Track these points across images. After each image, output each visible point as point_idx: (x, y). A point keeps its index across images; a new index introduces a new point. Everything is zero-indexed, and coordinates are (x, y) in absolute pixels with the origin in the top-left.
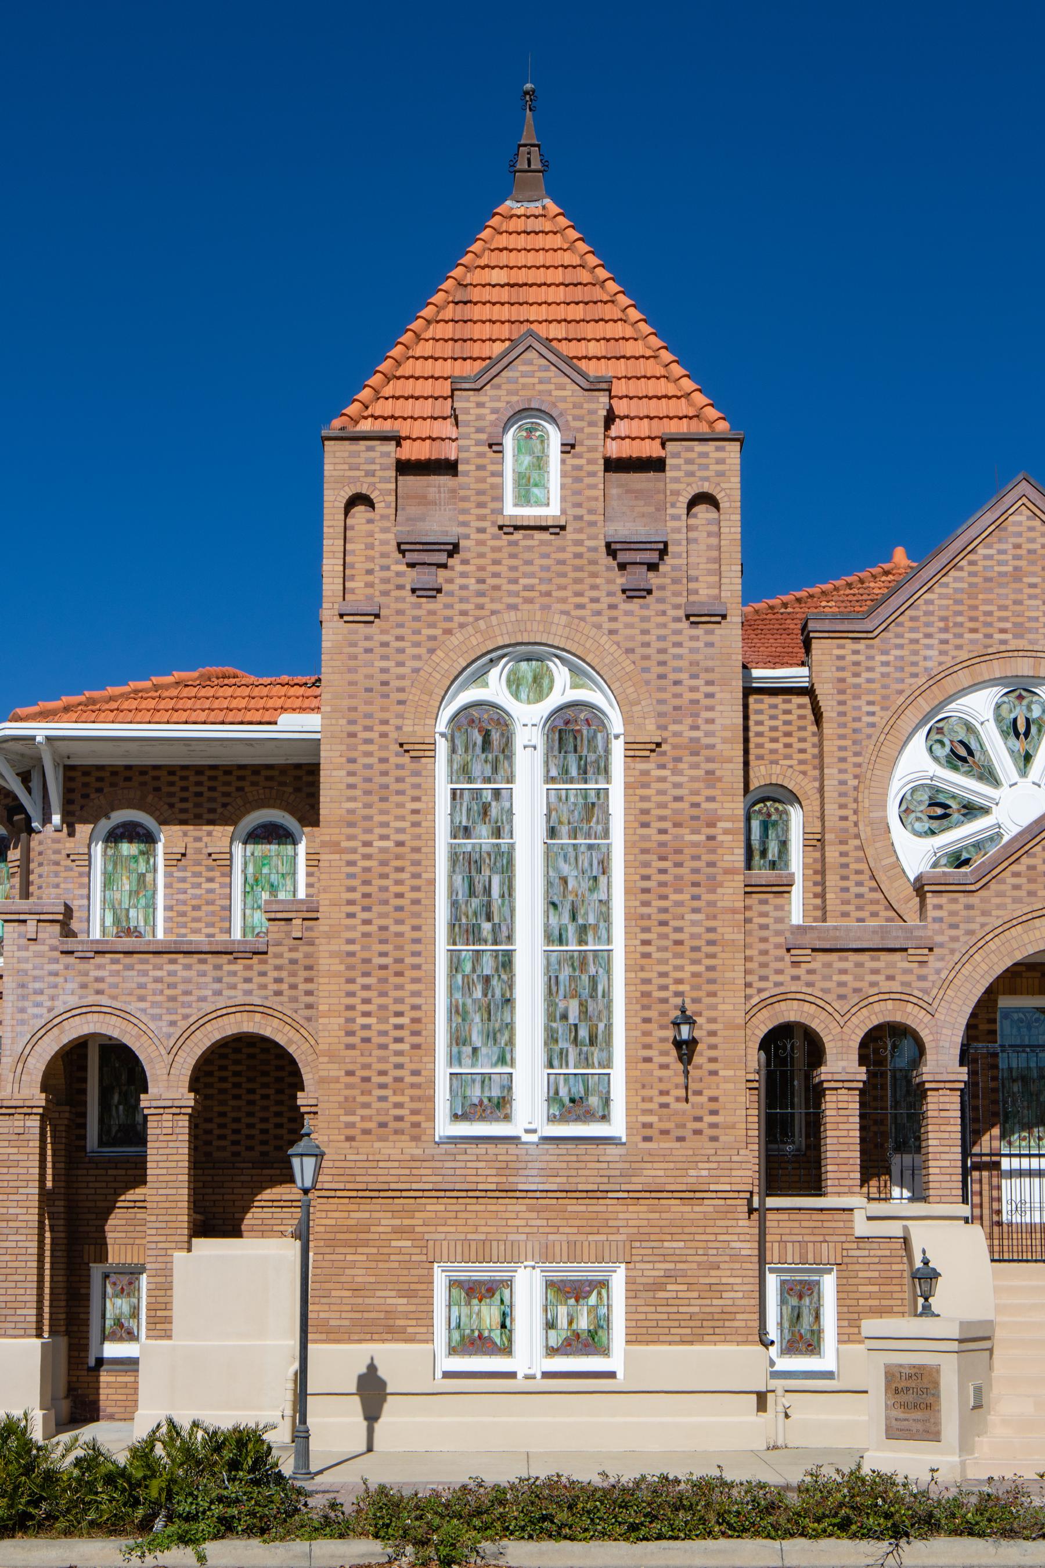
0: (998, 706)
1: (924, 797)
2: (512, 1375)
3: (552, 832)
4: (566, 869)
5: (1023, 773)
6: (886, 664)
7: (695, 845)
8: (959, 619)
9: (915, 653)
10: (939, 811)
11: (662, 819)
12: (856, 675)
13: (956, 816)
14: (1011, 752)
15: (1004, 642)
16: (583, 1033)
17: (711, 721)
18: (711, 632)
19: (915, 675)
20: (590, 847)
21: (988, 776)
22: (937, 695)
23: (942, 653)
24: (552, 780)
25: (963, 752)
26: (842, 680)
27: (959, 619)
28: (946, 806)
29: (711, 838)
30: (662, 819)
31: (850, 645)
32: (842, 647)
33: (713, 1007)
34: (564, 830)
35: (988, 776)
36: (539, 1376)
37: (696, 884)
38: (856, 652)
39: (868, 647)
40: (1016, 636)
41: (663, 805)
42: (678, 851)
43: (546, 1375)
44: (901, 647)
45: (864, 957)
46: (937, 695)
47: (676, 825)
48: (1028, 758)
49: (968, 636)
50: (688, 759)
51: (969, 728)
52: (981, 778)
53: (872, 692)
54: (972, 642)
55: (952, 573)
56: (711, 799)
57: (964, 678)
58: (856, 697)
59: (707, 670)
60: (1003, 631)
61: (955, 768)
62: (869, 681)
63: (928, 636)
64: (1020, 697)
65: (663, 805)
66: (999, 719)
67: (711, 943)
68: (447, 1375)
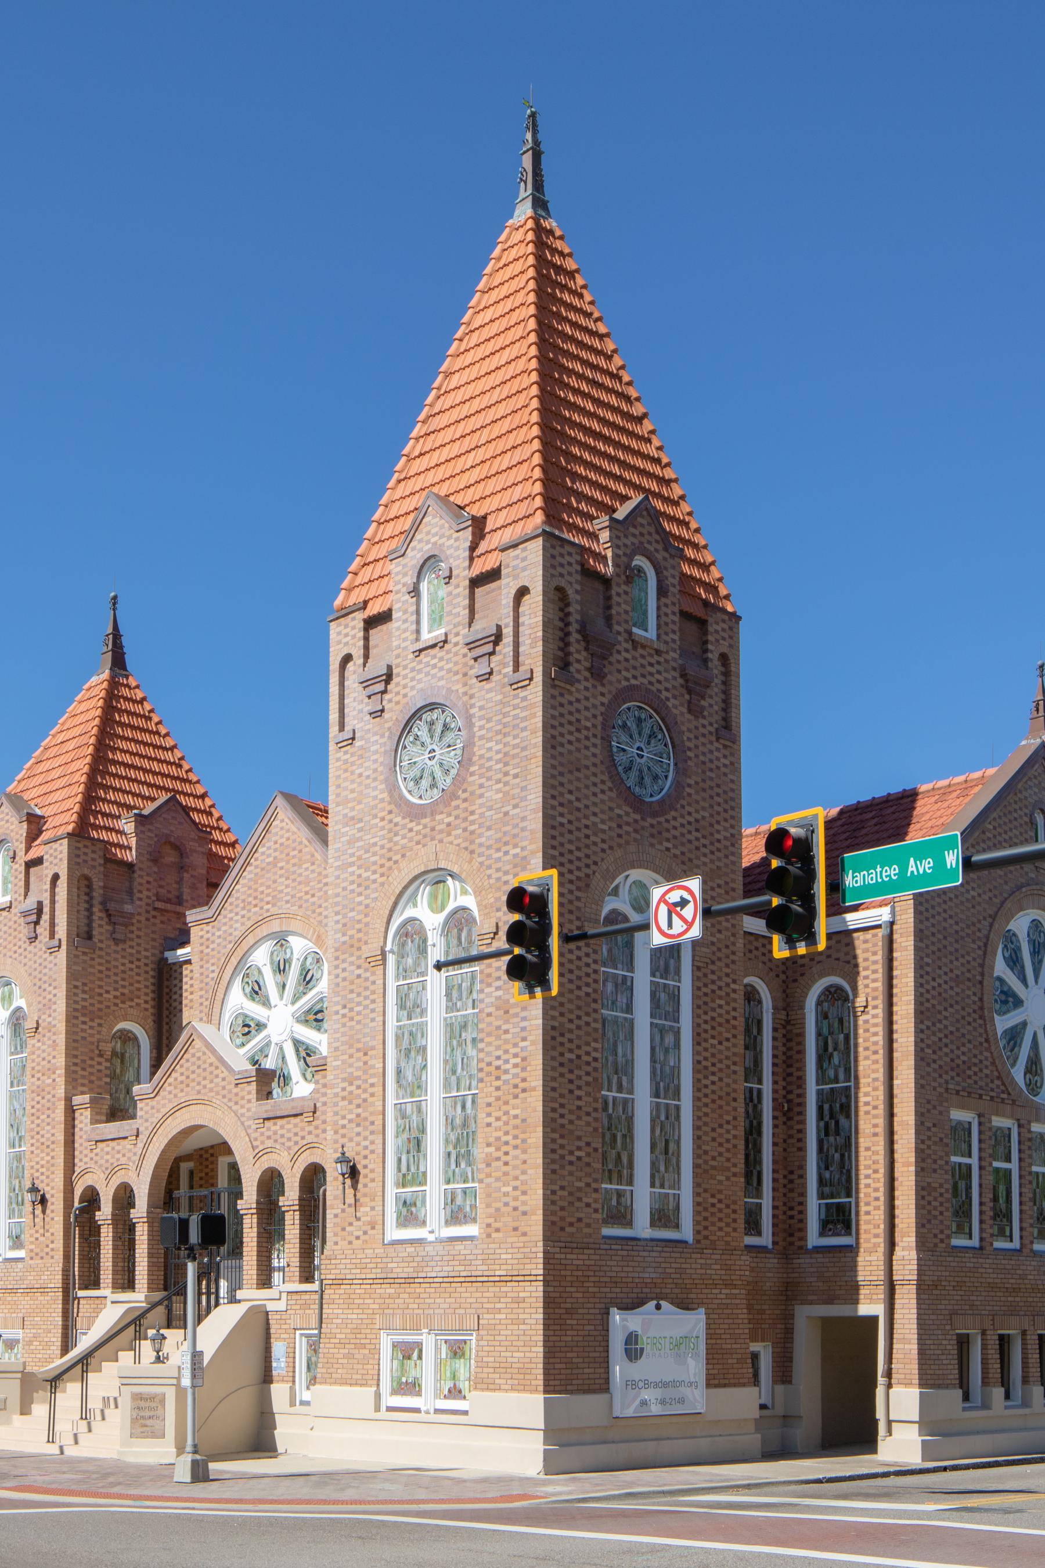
0: (272, 953)
1: (240, 1022)
2: (417, 1410)
3: (12, 1086)
4: (17, 1105)
5: (281, 997)
6: (219, 937)
7: (49, 1085)
8: (250, 899)
9: (231, 927)
10: (246, 1030)
11: (39, 1072)
12: (208, 947)
13: (253, 1032)
14: (277, 983)
15: (268, 911)
16: (20, 1199)
17: (55, 1011)
18: (56, 957)
19: (230, 942)
20: (23, 1090)
21: (266, 1003)
22: (239, 953)
23: (243, 924)
24: (12, 1054)
25: (257, 988)
26: (202, 952)
27: (250, 899)
28: (248, 1026)
29: (54, 1080)
30: (39, 1072)
31: (206, 928)
32: (202, 930)
33: (53, 1181)
34: (15, 1082)
35: (266, 1003)
36: (432, 1411)
37: (49, 1109)
38: (208, 932)
39: (213, 927)
40: (274, 905)
41: (39, 1064)
42: (43, 1090)
43: (437, 1411)
44: (225, 924)
45: (112, 1144)
46: (239, 953)
47: (43, 1075)
48: (284, 986)
49: (254, 910)
50: (48, 1035)
51: (260, 972)
52: (264, 1004)
53: (213, 957)
54: (255, 913)
55: (248, 868)
56: (54, 1057)
57: (250, 940)
58: (207, 962)
59: (55, 980)
60: (268, 903)
61: (253, 999)
62: (213, 950)
63: (237, 914)
64: (282, 945)
65: (39, 1064)
66: (272, 962)
67: (53, 1143)
68: (390, 1409)
